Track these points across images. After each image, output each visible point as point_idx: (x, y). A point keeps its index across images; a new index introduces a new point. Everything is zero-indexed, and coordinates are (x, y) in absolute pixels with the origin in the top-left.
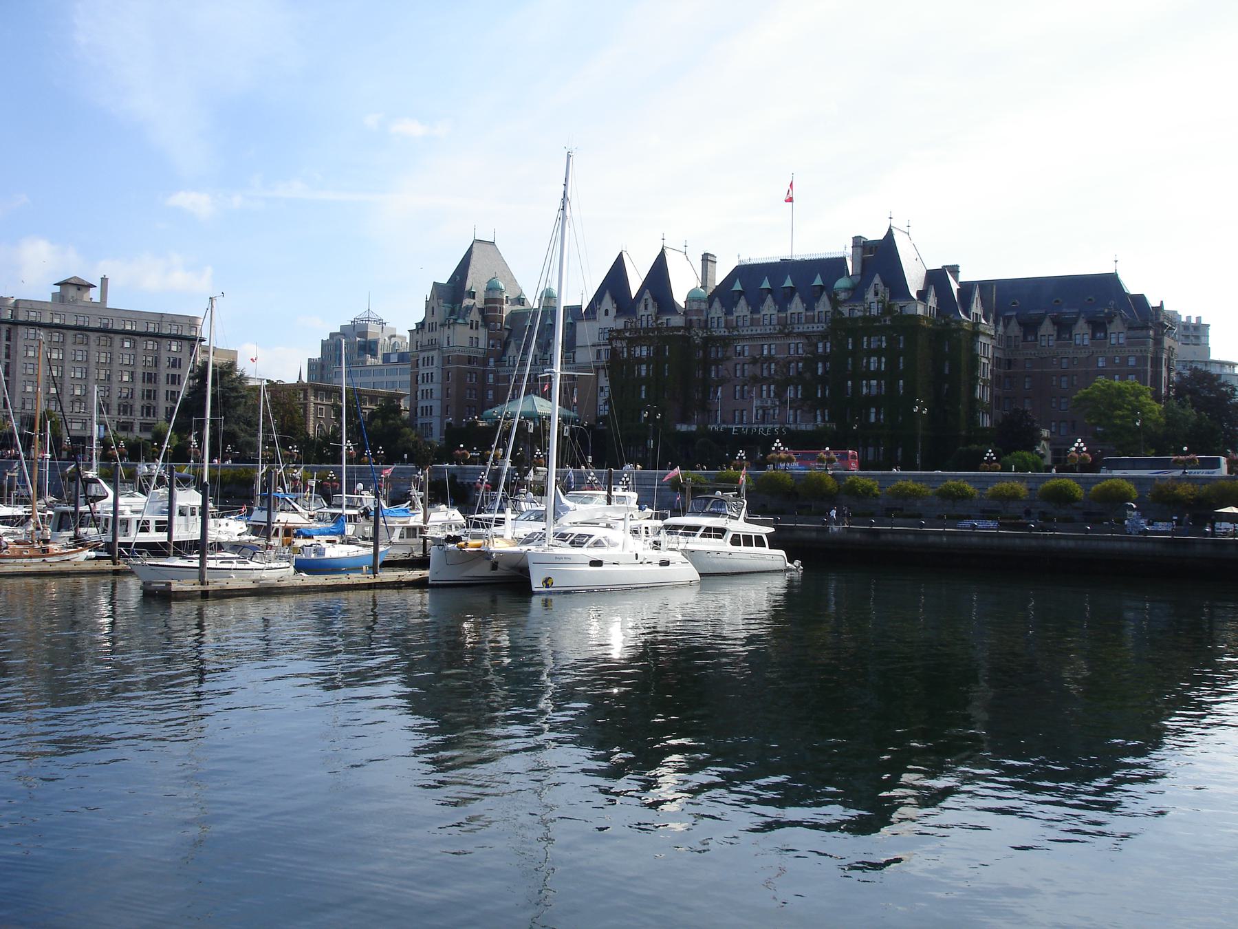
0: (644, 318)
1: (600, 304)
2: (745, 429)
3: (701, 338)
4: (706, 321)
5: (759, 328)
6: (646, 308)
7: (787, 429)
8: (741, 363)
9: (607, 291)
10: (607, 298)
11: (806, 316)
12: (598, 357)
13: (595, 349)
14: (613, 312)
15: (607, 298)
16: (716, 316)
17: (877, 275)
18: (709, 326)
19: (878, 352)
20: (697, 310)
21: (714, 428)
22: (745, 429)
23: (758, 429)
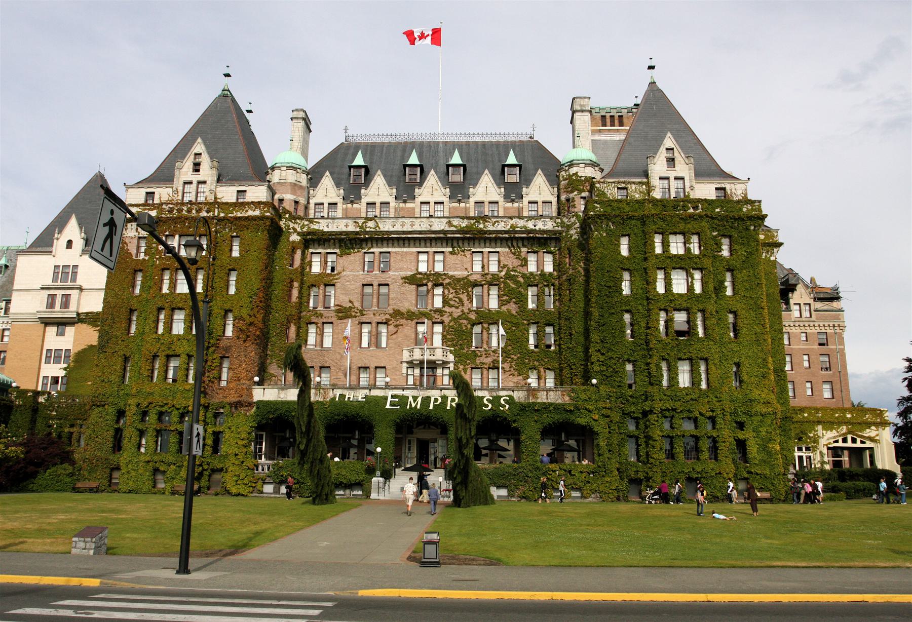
0: (192, 188)
1: (60, 232)
2: (415, 398)
3: (299, 234)
4: (306, 208)
5: (417, 222)
6: (197, 167)
7: (510, 401)
8: (376, 284)
9: (74, 215)
10: (73, 223)
11: (505, 209)
12: (51, 304)
13: (46, 293)
14: (79, 244)
15: (73, 223)
16: (326, 202)
17: (669, 134)
18: (312, 216)
19: (685, 263)
20: (295, 184)
21: (342, 396)
22: (415, 398)
23: (445, 398)
